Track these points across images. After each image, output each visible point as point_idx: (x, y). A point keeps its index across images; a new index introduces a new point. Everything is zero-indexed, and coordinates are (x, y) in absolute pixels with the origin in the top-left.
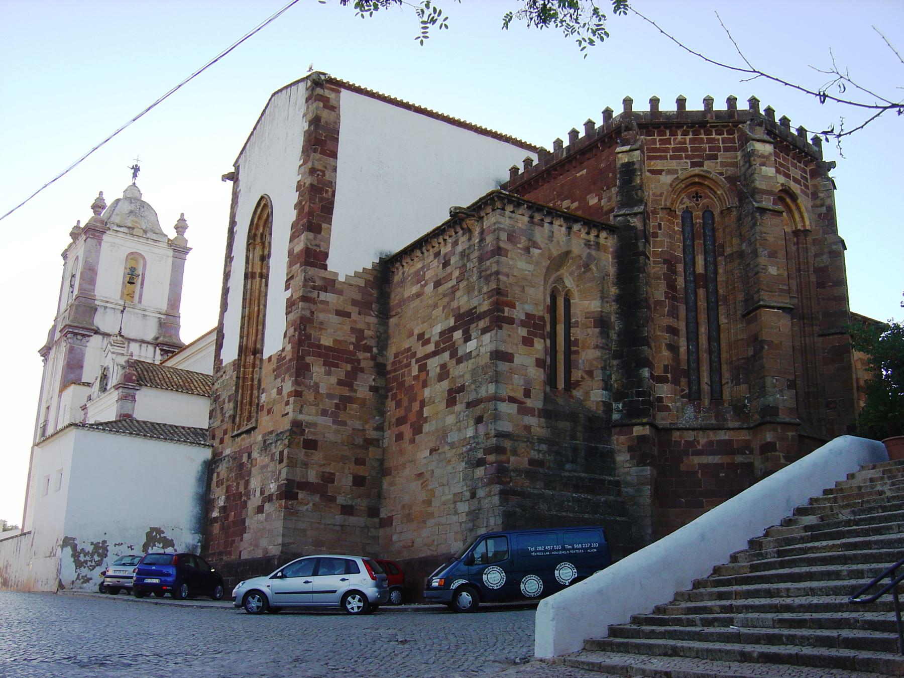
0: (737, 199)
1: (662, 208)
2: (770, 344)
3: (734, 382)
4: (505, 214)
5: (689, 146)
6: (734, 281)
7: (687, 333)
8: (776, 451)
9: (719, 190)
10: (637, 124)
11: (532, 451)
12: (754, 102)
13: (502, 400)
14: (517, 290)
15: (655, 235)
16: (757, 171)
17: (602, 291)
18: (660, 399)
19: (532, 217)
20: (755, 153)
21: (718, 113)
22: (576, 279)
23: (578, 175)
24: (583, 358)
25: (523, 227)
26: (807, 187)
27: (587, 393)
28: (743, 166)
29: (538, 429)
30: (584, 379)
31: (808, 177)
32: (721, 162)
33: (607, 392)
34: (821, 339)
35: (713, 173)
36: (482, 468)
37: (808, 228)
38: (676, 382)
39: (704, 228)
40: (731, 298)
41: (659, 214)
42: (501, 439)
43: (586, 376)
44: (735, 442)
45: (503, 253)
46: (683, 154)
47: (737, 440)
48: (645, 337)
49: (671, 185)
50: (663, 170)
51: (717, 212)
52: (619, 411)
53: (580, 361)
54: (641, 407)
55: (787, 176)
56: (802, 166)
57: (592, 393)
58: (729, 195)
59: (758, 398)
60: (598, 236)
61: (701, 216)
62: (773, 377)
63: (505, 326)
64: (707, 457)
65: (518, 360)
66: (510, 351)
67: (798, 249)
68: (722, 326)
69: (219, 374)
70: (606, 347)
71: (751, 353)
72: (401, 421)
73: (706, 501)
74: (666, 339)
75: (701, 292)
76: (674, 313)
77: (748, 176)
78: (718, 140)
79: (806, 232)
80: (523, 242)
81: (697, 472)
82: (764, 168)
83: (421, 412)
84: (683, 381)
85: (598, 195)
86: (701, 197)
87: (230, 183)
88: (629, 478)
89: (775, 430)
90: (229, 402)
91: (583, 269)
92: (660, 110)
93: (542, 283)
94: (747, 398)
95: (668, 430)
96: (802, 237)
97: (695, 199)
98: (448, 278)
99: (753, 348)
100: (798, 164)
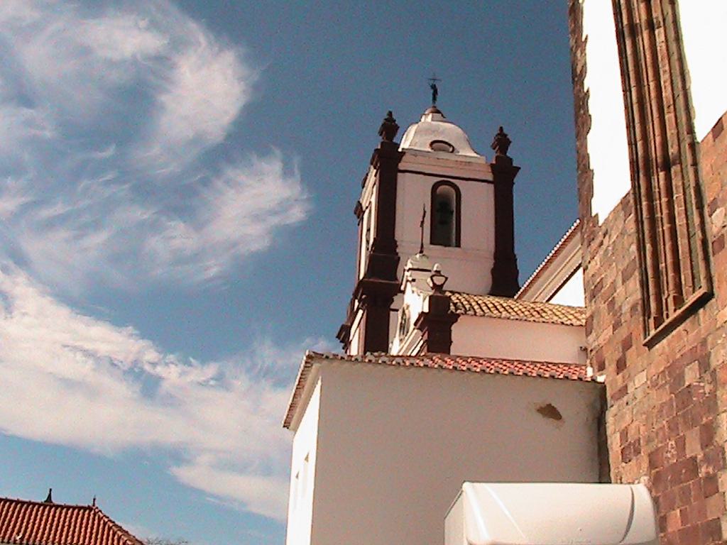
69: (594, 245)
90: (624, 282)
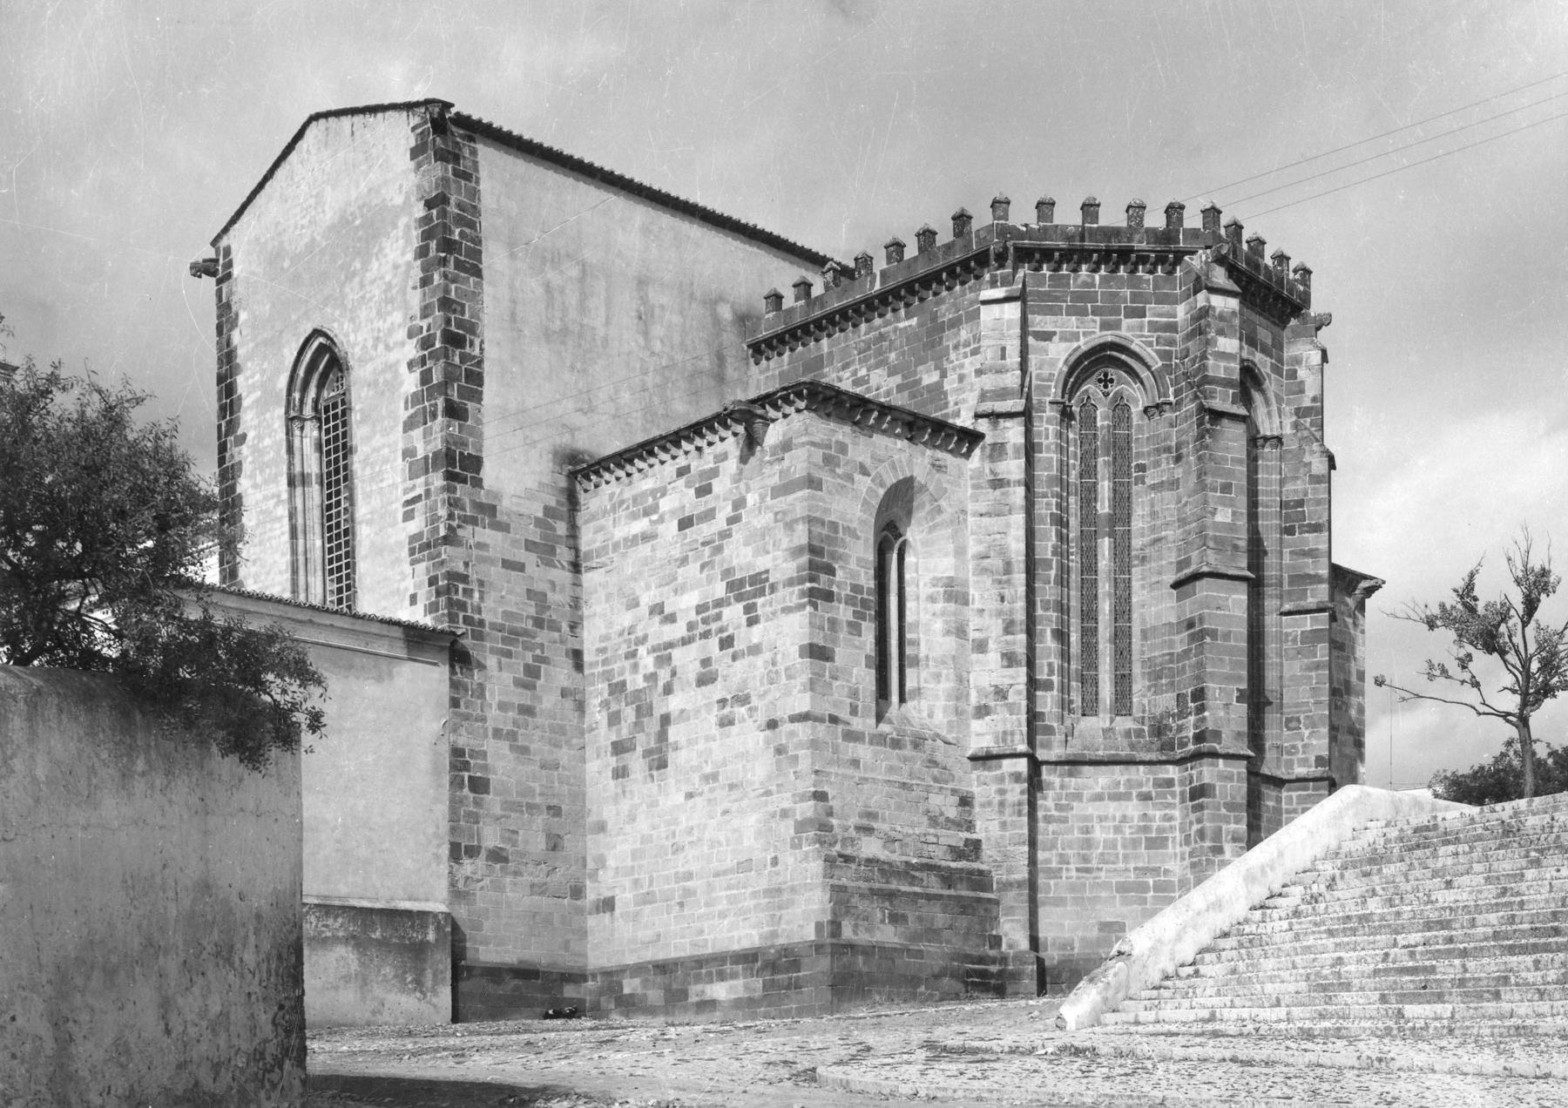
12: (1212, 214)
50: (1054, 333)
72: (619, 748)
83: (662, 736)
86: (1112, 381)
87: (209, 283)
98: (709, 515)
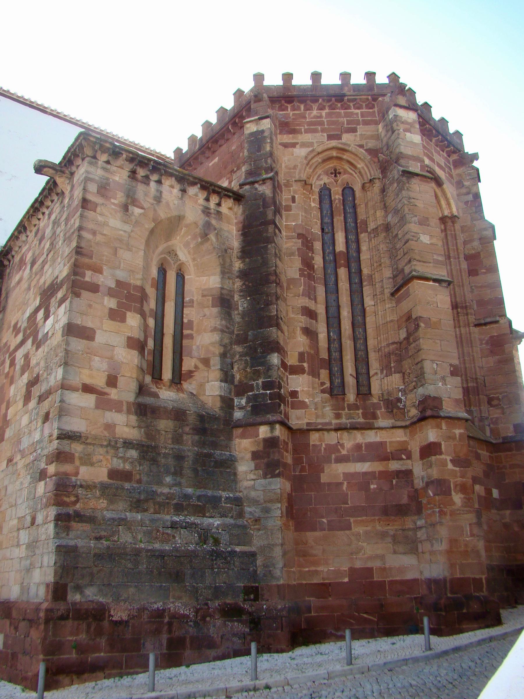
0: (379, 171)
1: (295, 181)
2: (428, 322)
3: (385, 372)
4: (97, 163)
5: (325, 120)
6: (380, 256)
7: (327, 318)
8: (441, 453)
9: (359, 164)
10: (269, 97)
11: (115, 459)
13: (73, 389)
14: (106, 252)
15: (288, 208)
16: (401, 136)
17: (223, 265)
18: (294, 394)
19: (133, 172)
20: (398, 118)
21: (357, 88)
22: (192, 251)
23: (210, 165)
24: (198, 344)
25: (121, 181)
26: (451, 176)
27: (202, 386)
28: (386, 135)
29: (126, 429)
30: (199, 369)
31: (452, 167)
32: (361, 135)
33: (226, 385)
34: (477, 329)
35: (352, 145)
36: (43, 483)
37: (455, 213)
38: (314, 373)
39: (344, 205)
40: (377, 276)
41: (292, 186)
42: (66, 442)
43: (200, 365)
44: (388, 444)
45: (89, 205)
46: (319, 128)
47: (391, 442)
48: (274, 316)
49: (306, 158)
50: (297, 143)
51: (357, 188)
52: (241, 408)
53: (194, 347)
54: (269, 402)
55: (432, 160)
56: (446, 156)
57: (208, 386)
58: (370, 168)
59: (415, 388)
60: (219, 204)
61: (340, 192)
62: (433, 361)
63: (85, 294)
64: (354, 464)
65: (100, 338)
66: (90, 325)
67: (446, 235)
68: (367, 309)
70: (227, 330)
71: (403, 334)
73: (354, 521)
74: (301, 322)
75: (343, 272)
76: (310, 293)
77: (390, 143)
78: (357, 114)
79: (453, 218)
80: (120, 198)
81: (341, 484)
82: (408, 134)
84: (324, 373)
85: (229, 178)
86: (340, 173)
88: (253, 494)
89: (439, 427)
91: (200, 240)
92: (293, 84)
93: (142, 247)
94: (400, 390)
95: (305, 432)
96: (450, 223)
97: (333, 175)
99: (405, 330)
100: (441, 152)
